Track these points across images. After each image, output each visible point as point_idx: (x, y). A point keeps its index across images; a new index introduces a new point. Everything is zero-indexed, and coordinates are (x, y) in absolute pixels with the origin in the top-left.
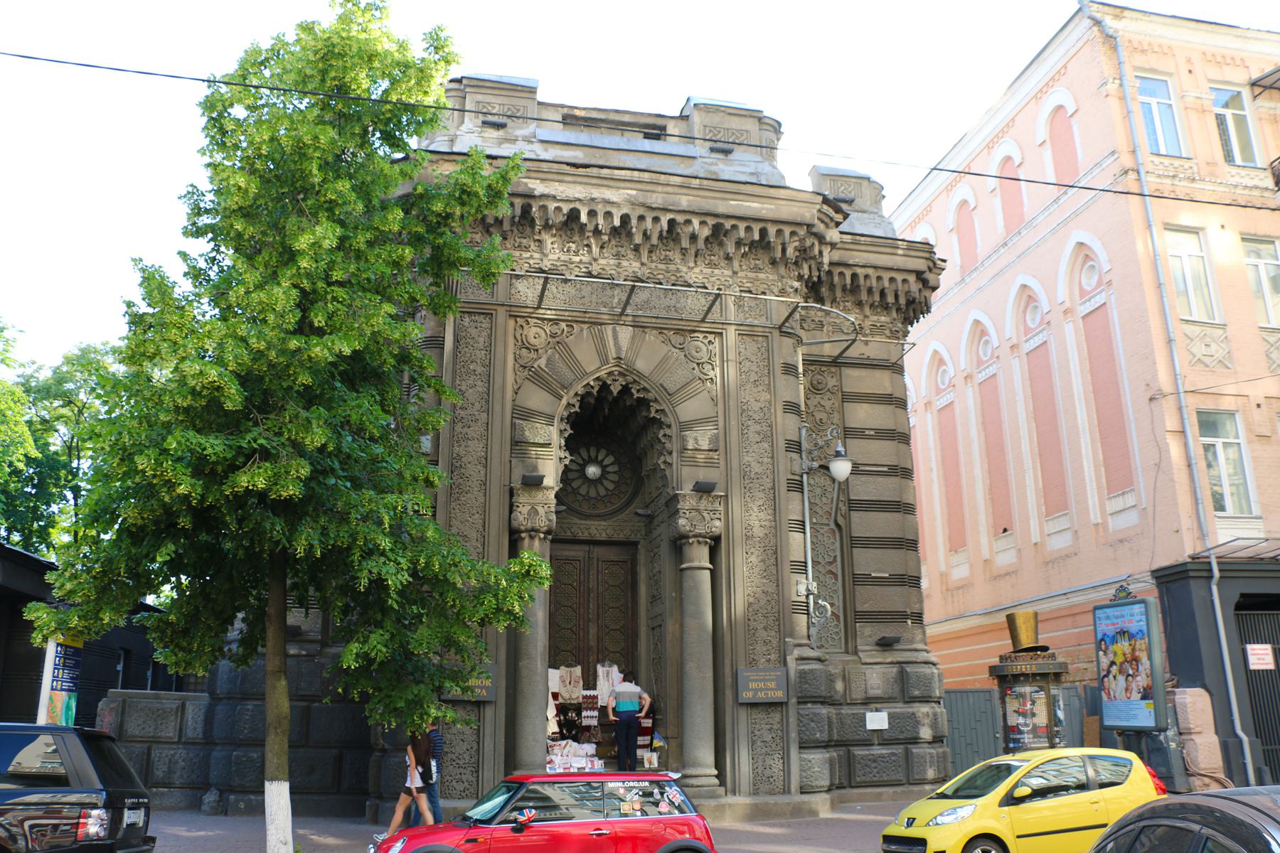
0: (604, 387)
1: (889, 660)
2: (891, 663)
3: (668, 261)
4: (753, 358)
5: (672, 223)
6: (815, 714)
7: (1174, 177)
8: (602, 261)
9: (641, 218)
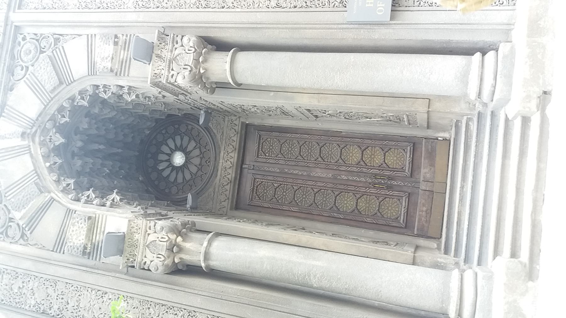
0: (57, 150)
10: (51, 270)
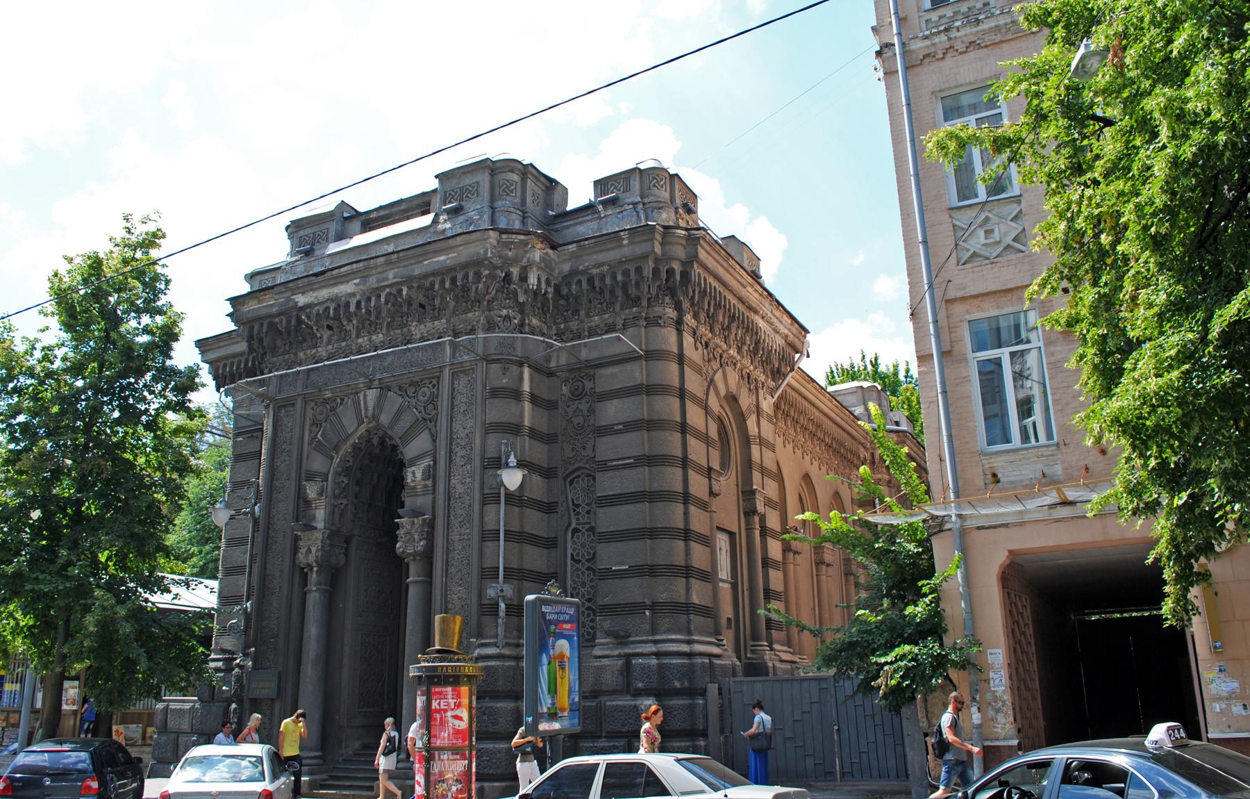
1: (616, 653)
2: (619, 656)
3: (406, 325)
4: (464, 391)
5: (390, 294)
6: (487, 708)
7: (946, 30)
8: (360, 340)
9: (369, 299)
10: (293, 475)
